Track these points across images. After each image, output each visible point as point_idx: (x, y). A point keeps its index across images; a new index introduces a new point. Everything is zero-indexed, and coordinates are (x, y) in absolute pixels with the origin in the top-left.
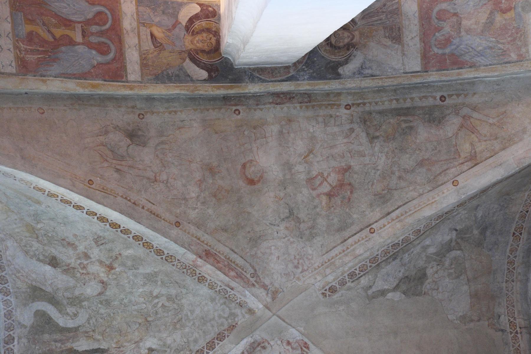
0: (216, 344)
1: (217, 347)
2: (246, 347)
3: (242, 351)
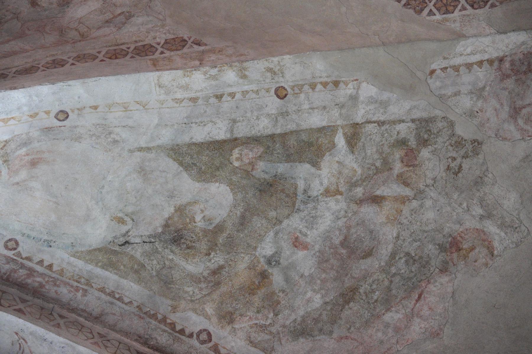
0: (459, 7)
1: (457, 13)
2: (515, 54)
3: (501, 54)
